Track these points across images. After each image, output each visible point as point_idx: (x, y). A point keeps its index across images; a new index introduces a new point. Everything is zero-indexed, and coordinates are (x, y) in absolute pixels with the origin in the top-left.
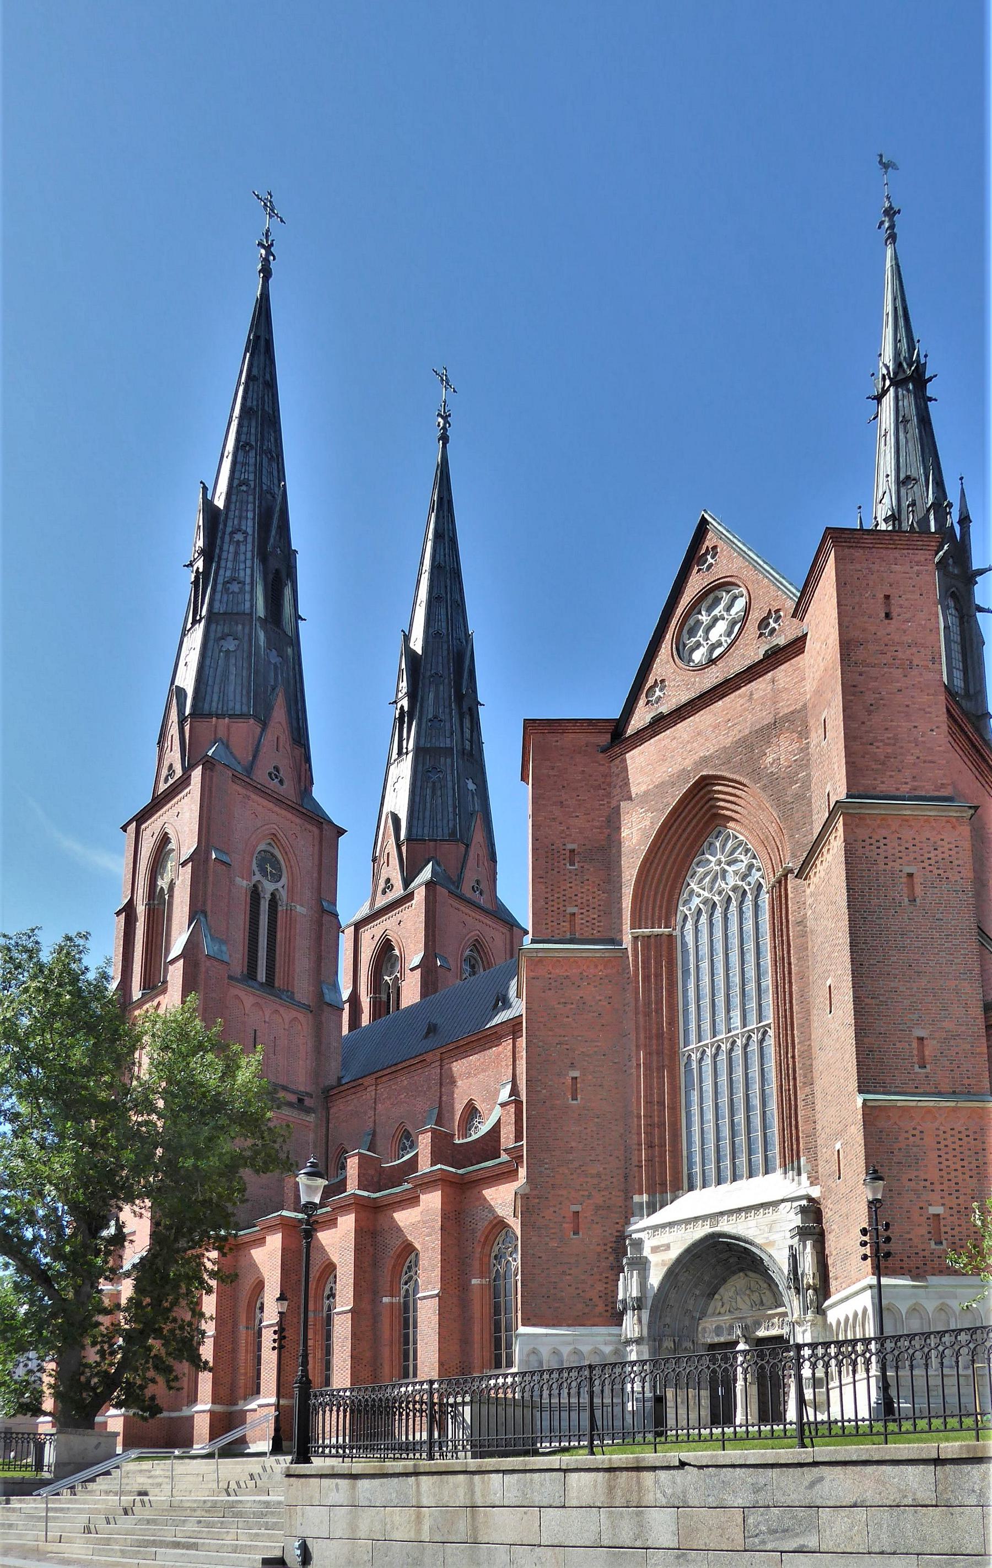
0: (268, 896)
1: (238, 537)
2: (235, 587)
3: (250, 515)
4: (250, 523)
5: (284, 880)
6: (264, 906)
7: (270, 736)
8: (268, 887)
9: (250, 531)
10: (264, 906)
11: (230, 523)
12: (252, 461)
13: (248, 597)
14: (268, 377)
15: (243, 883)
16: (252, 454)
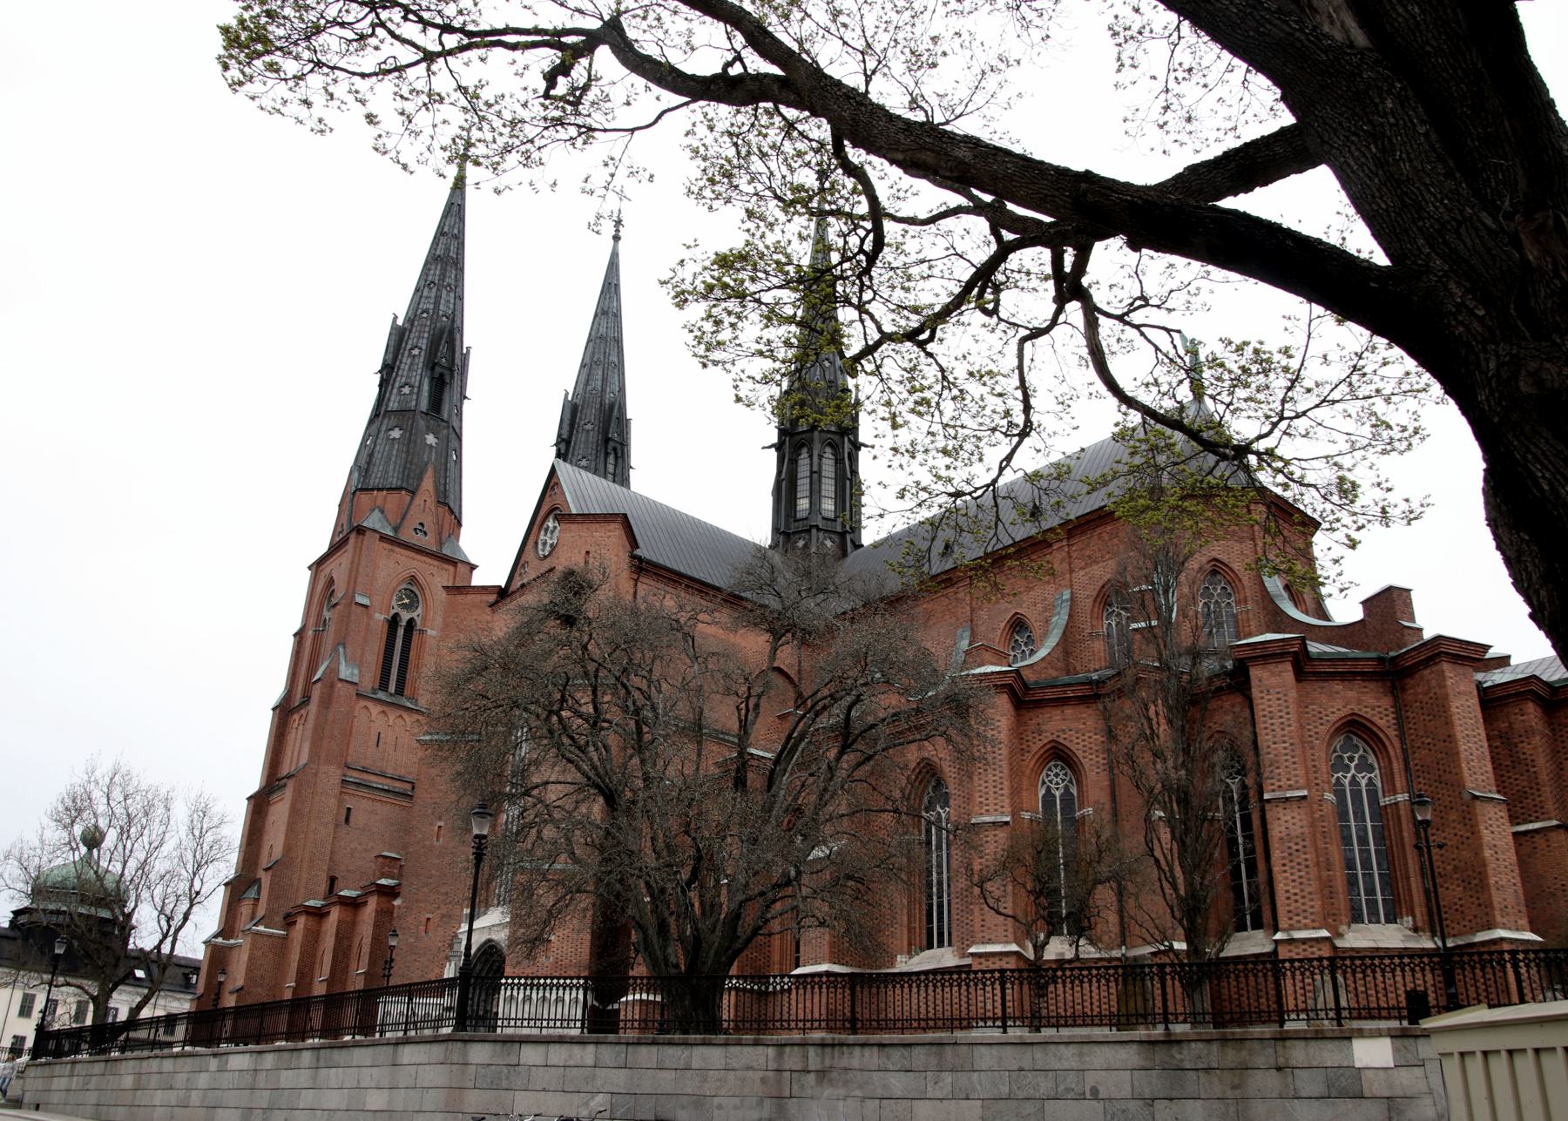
0: (404, 623)
1: (416, 352)
2: (406, 390)
3: (426, 335)
4: (425, 341)
5: (419, 610)
6: (401, 632)
7: (418, 500)
8: (405, 616)
9: (424, 347)
10: (401, 632)
11: (410, 342)
12: (433, 295)
13: (415, 397)
14: (456, 231)
15: (380, 617)
16: (434, 290)
